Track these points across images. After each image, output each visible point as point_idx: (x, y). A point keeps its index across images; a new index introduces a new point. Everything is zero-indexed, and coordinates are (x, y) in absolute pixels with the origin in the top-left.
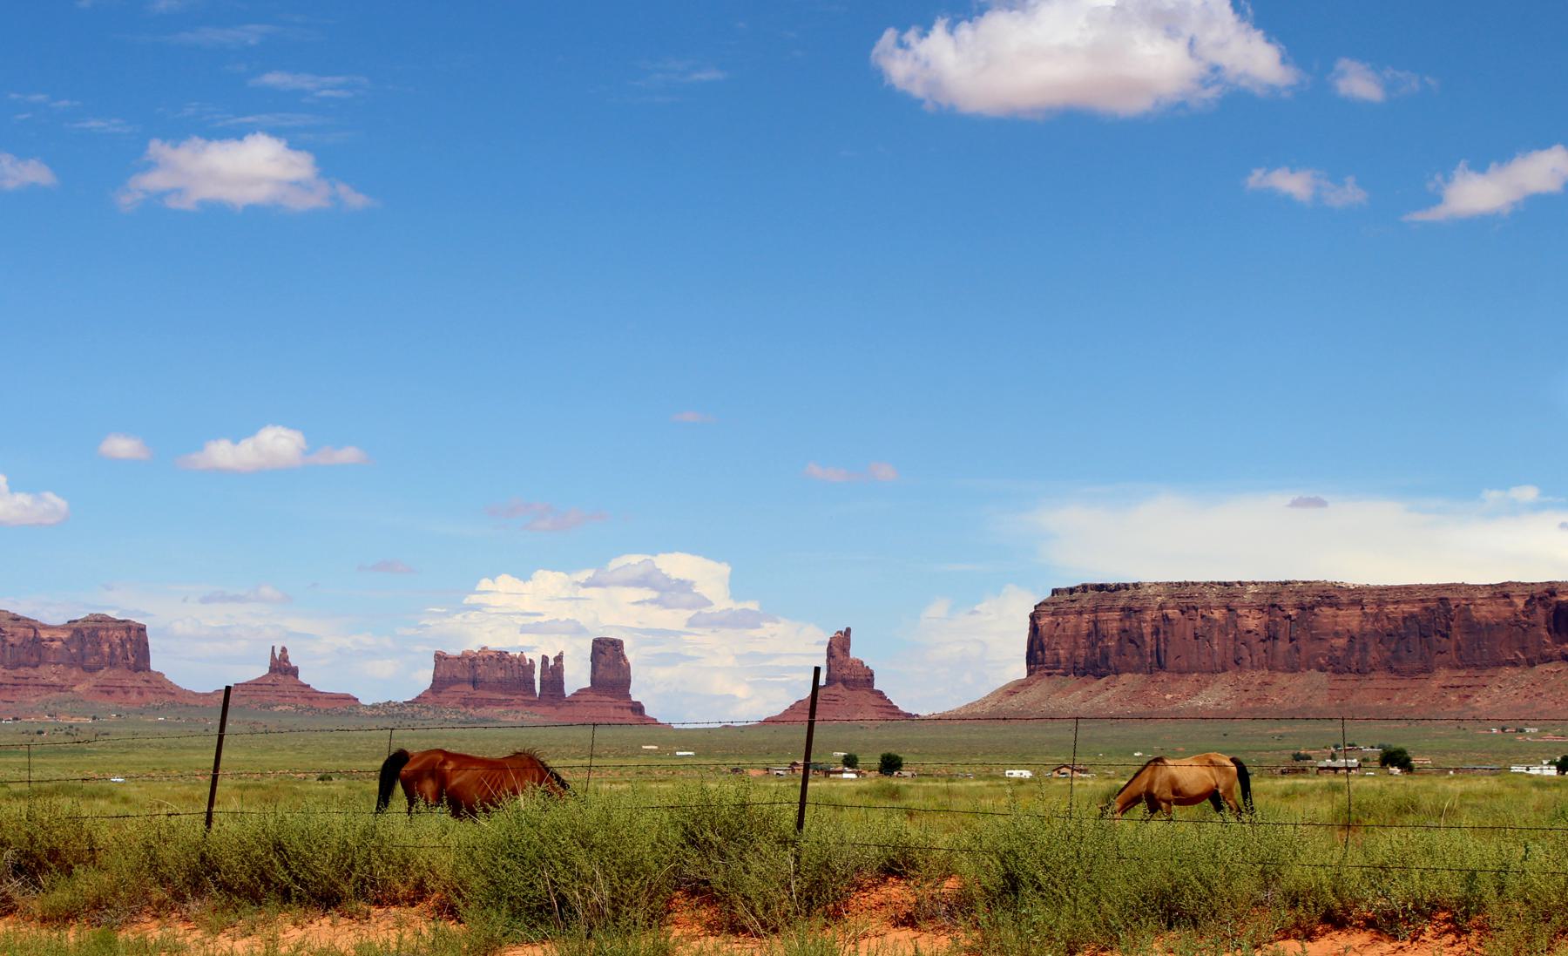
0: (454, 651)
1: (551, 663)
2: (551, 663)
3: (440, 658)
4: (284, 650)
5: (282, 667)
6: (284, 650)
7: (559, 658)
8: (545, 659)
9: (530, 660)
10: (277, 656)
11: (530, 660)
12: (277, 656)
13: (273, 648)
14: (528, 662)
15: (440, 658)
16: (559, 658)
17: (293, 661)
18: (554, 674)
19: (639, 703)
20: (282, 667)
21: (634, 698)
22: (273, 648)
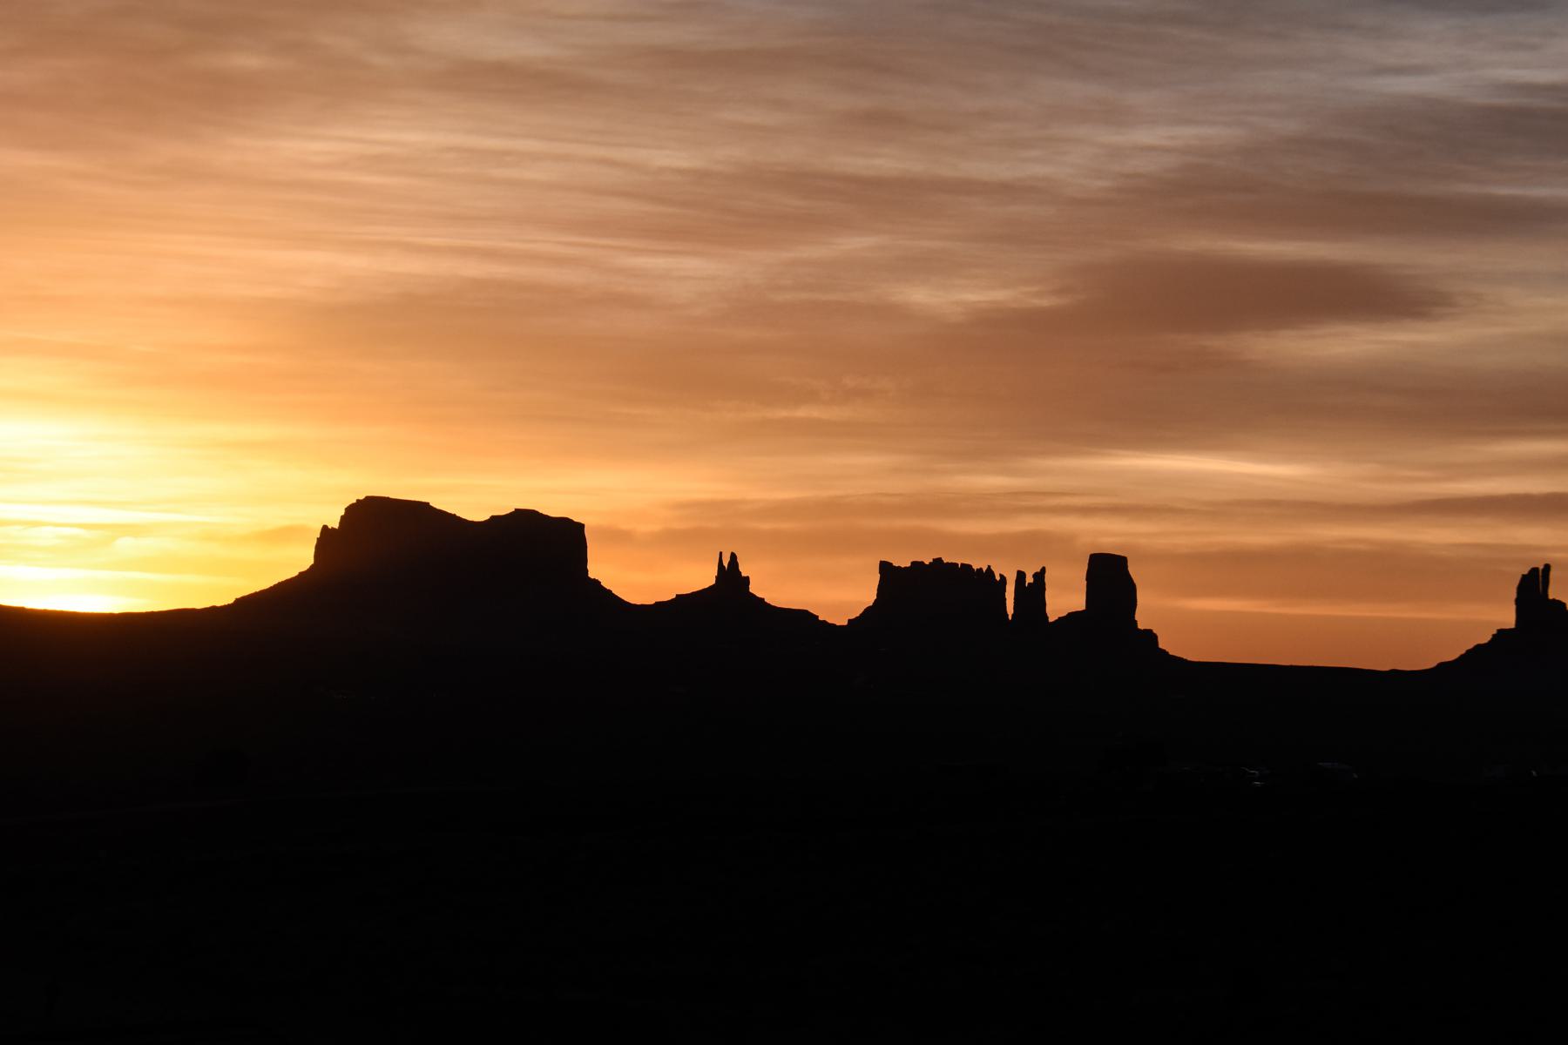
0: (902, 561)
1: (1029, 579)
2: (1029, 579)
3: (885, 567)
4: (733, 557)
5: (730, 577)
6: (733, 557)
7: (1040, 576)
8: (1021, 576)
9: (1001, 576)
10: (726, 566)
11: (1001, 576)
12: (726, 566)
13: (721, 553)
14: (998, 578)
15: (885, 567)
16: (1040, 576)
17: (744, 570)
18: (1033, 592)
19: (1151, 631)
20: (730, 577)
21: (1141, 626)
22: (721, 553)
